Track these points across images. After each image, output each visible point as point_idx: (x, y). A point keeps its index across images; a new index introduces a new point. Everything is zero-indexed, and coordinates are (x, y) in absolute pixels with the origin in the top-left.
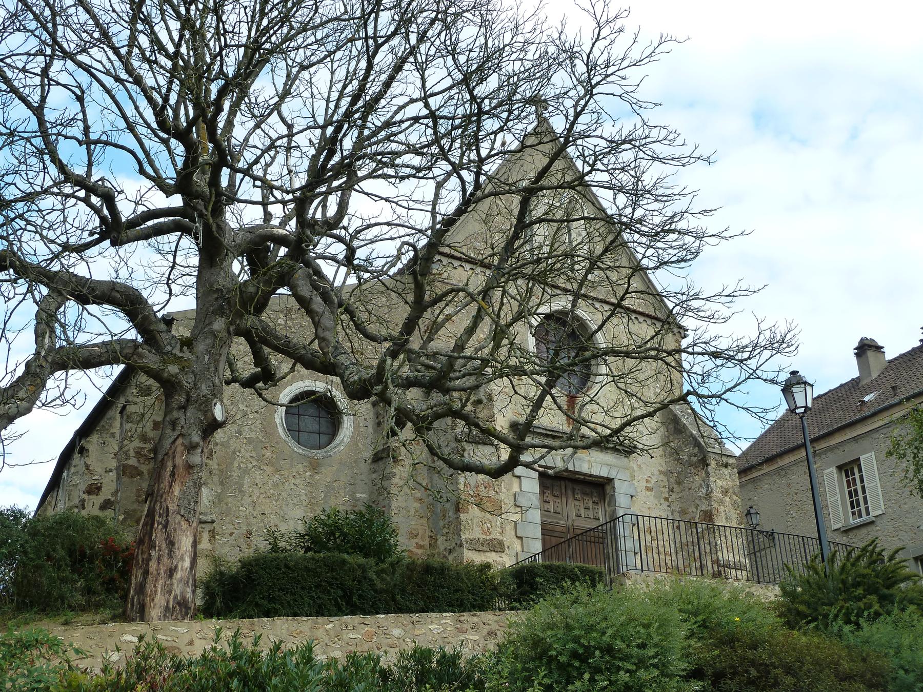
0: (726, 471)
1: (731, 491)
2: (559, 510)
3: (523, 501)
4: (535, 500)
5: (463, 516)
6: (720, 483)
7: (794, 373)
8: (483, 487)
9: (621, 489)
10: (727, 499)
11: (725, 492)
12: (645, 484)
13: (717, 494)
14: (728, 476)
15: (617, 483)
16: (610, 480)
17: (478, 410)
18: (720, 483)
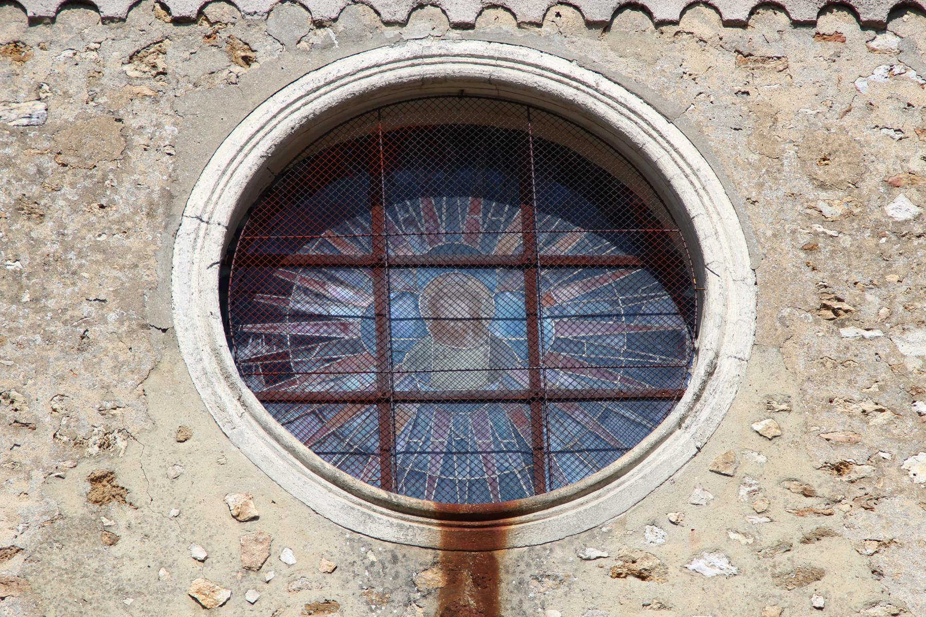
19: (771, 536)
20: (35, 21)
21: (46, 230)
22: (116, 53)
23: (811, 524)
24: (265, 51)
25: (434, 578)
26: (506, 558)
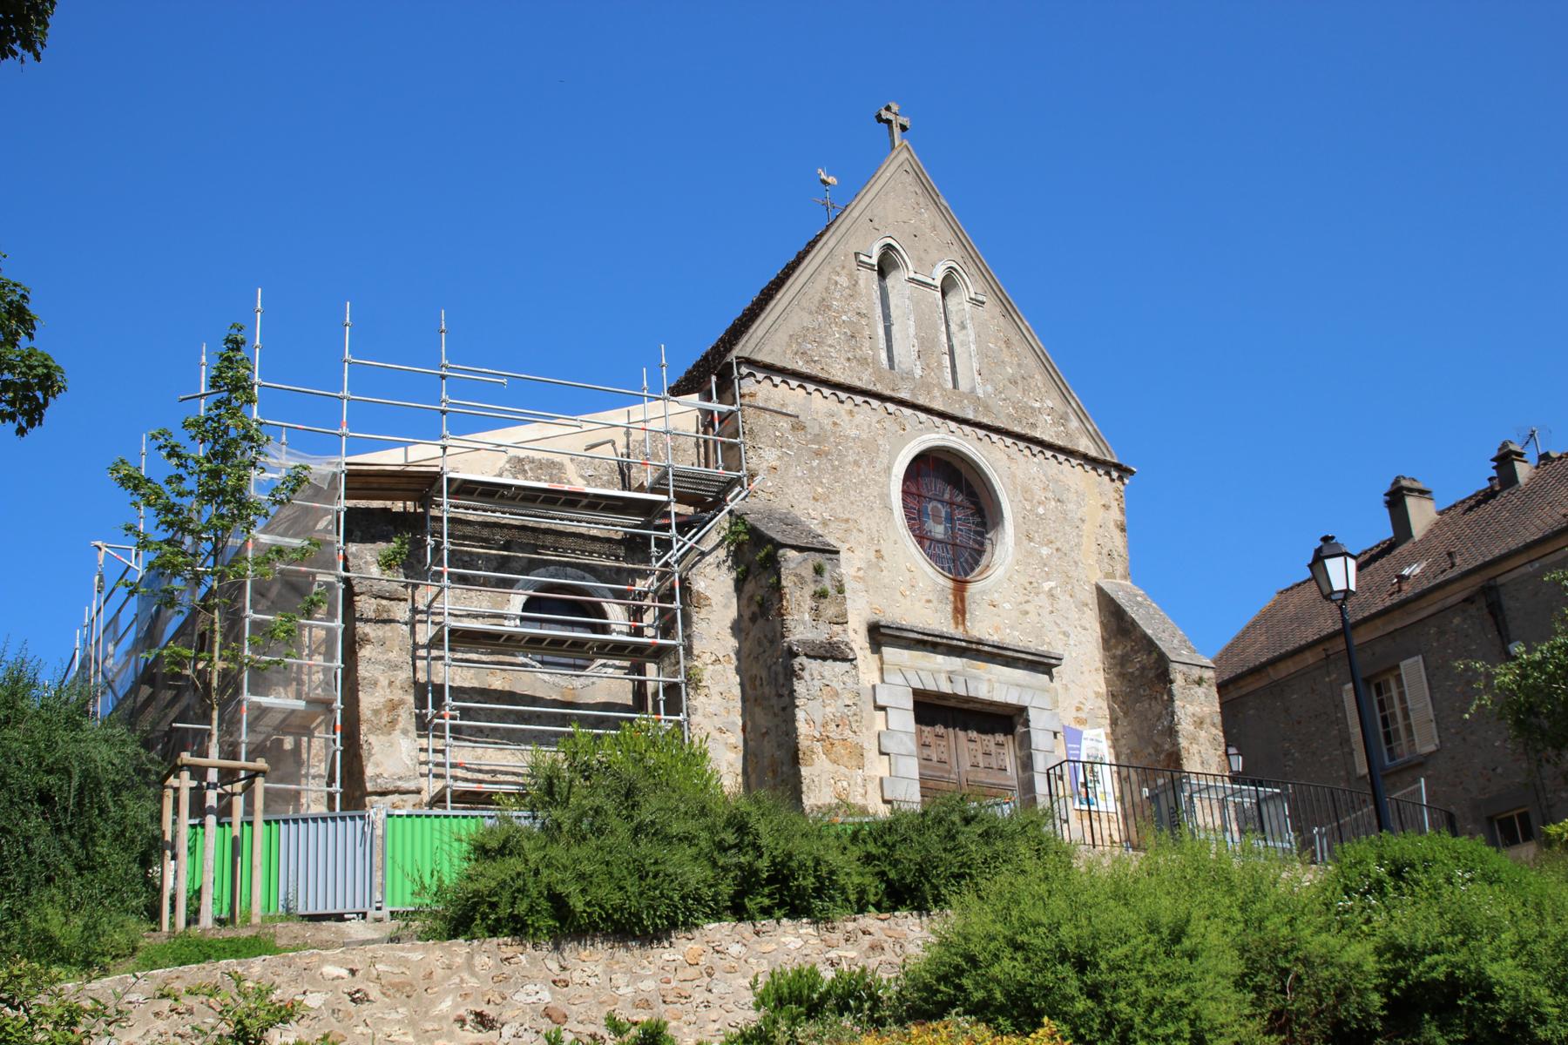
0: (1200, 691)
1: (1208, 721)
2: (944, 757)
3: (888, 745)
4: (910, 745)
5: (804, 771)
6: (1190, 709)
7: (1326, 539)
8: (834, 725)
9: (1039, 723)
10: (1203, 733)
11: (1200, 723)
12: (1075, 714)
13: (1185, 726)
14: (1203, 698)
15: (1032, 714)
16: (1022, 710)
17: (821, 607)
18: (1190, 709)
19: (1019, 600)
20: (856, 405)
21: (861, 471)
22: (875, 420)
23: (1027, 598)
24: (908, 427)
25: (951, 598)
26: (967, 595)
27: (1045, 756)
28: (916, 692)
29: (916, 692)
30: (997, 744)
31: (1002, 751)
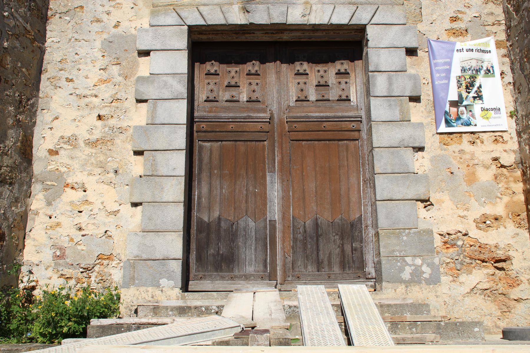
12: (448, 25)
15: (370, 31)
16: (361, 29)
27: (390, 79)
28: (192, 30)
29: (192, 30)
30: (339, 73)
31: (343, 81)
